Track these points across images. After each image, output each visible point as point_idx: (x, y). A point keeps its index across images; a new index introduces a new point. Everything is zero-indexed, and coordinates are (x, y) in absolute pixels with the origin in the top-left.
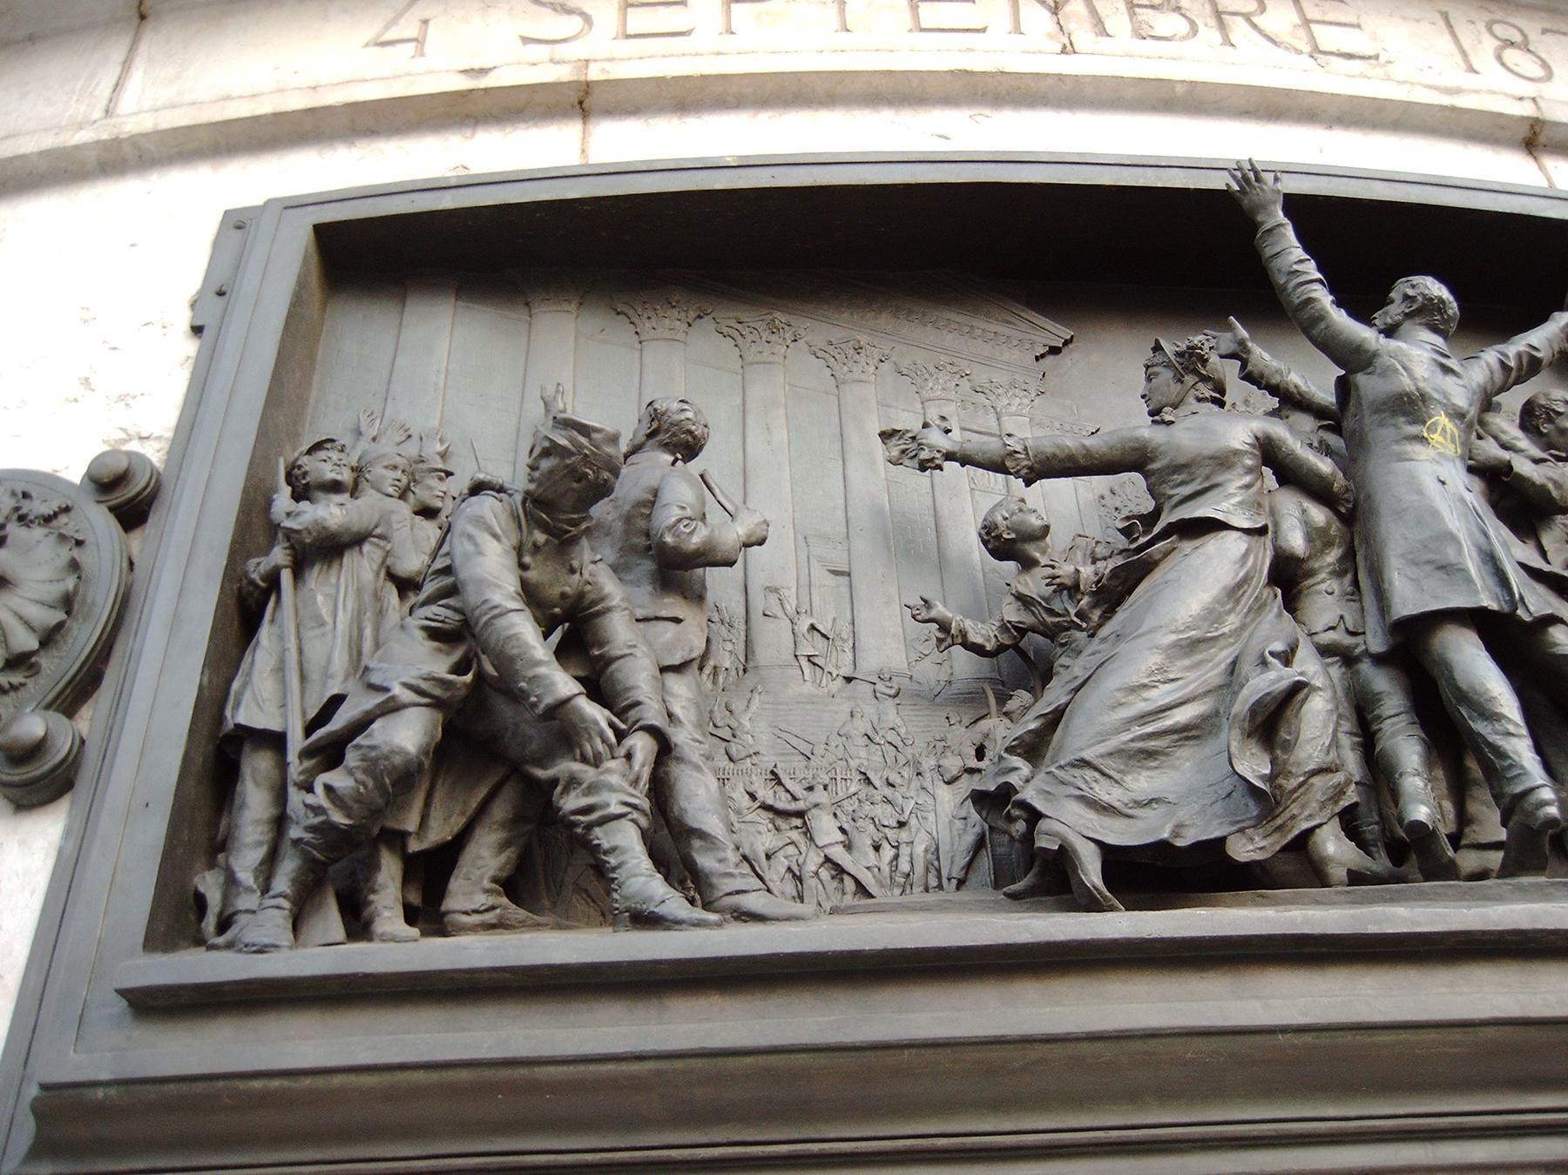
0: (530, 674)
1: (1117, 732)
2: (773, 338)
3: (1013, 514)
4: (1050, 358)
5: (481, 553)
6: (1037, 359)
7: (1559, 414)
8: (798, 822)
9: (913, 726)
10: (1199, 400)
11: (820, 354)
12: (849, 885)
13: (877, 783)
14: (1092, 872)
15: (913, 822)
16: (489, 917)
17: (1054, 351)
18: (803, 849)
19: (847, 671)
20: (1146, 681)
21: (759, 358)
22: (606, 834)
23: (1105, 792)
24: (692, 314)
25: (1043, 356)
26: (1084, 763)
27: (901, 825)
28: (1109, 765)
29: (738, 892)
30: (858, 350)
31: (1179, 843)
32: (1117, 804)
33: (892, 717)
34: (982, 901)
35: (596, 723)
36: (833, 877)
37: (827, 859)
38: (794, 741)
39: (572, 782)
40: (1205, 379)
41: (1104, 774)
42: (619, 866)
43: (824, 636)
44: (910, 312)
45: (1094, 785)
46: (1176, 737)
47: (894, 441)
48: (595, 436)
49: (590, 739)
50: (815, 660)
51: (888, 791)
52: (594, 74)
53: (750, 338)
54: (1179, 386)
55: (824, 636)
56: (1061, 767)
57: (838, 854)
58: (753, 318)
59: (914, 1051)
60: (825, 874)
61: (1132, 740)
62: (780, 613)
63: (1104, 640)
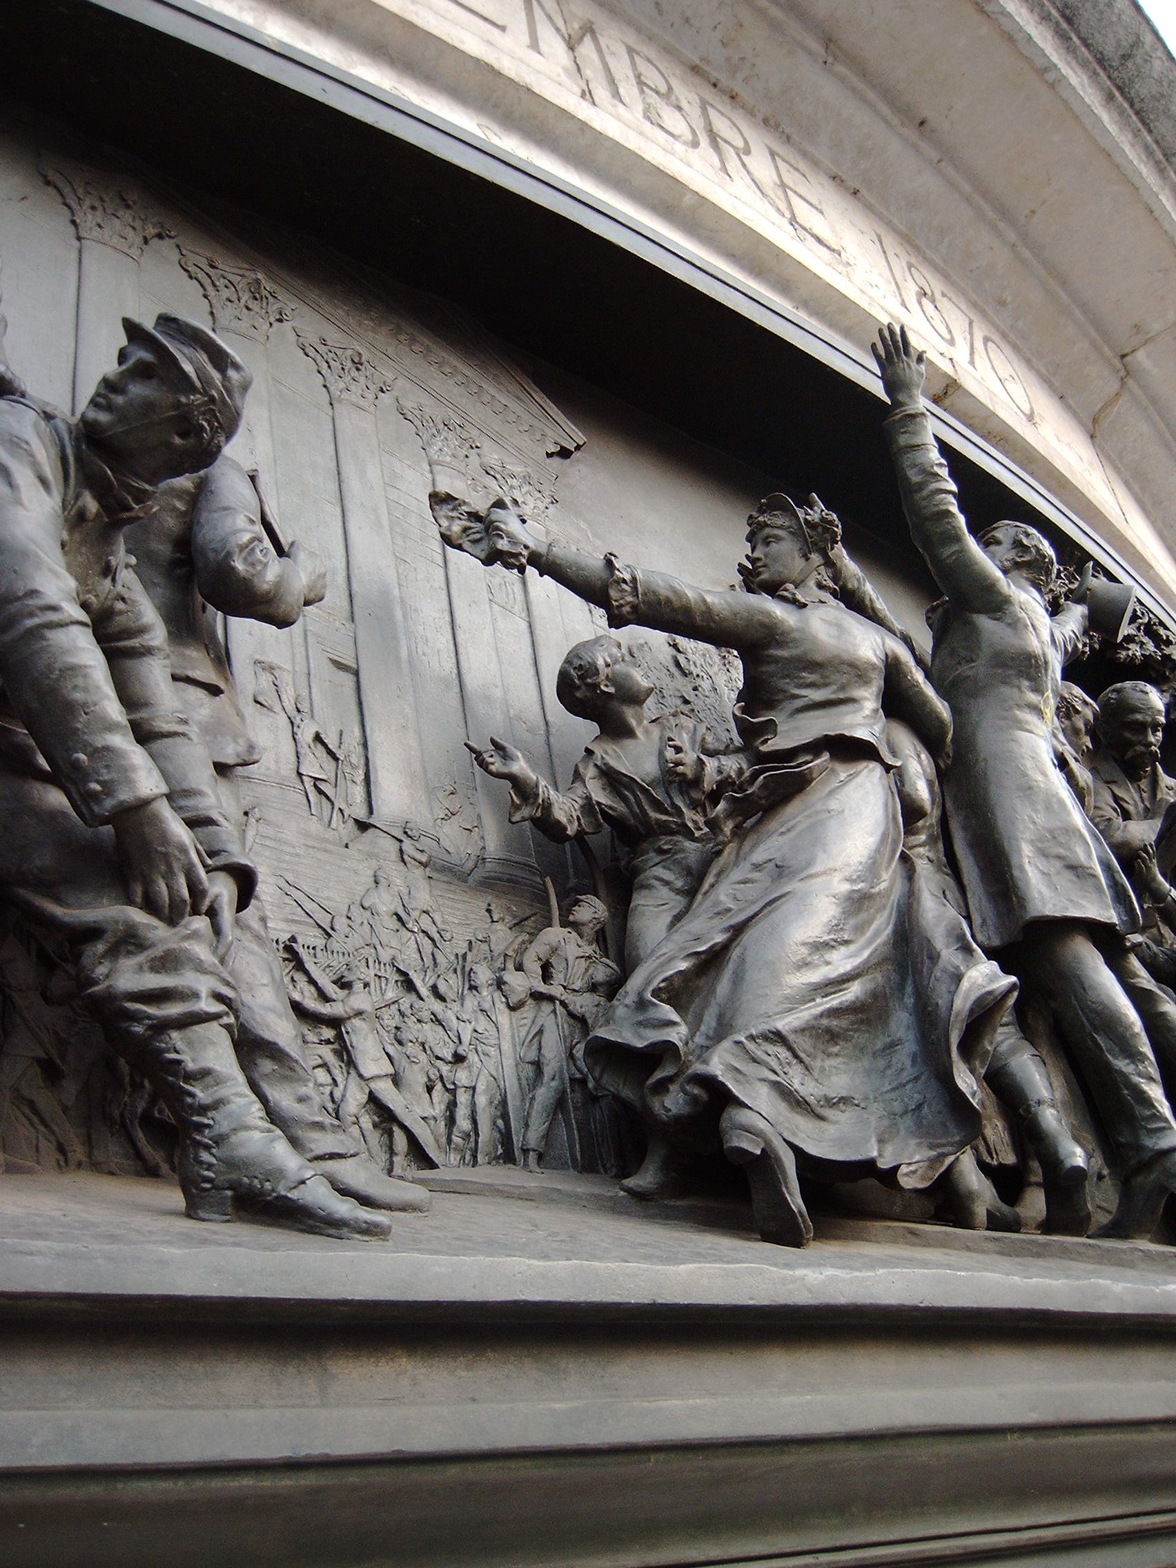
2: (255, 305)
3: (616, 662)
4: (557, 460)
5: (18, 502)
7: (1077, 712)
8: (328, 1033)
9: (464, 919)
11: (312, 353)
13: (424, 991)
15: (473, 1058)
17: (564, 453)
18: (339, 1079)
19: (361, 813)
21: (235, 324)
22: (190, 1044)
26: (778, 1037)
27: (459, 1059)
28: (803, 1044)
29: (333, 1156)
30: (358, 365)
32: (811, 1100)
33: (423, 896)
34: (598, 1197)
35: (183, 849)
36: (375, 1126)
37: (373, 1099)
38: (309, 905)
39: (130, 941)
42: (217, 1104)
43: (330, 753)
44: (413, 340)
47: (445, 510)
48: (232, 373)
49: (169, 876)
50: (322, 786)
51: (437, 1006)
53: (226, 293)
55: (330, 753)
56: (752, 1038)
57: (385, 1090)
58: (230, 268)
59: (662, 1456)
60: (366, 1121)
62: (278, 708)
63: (757, 867)
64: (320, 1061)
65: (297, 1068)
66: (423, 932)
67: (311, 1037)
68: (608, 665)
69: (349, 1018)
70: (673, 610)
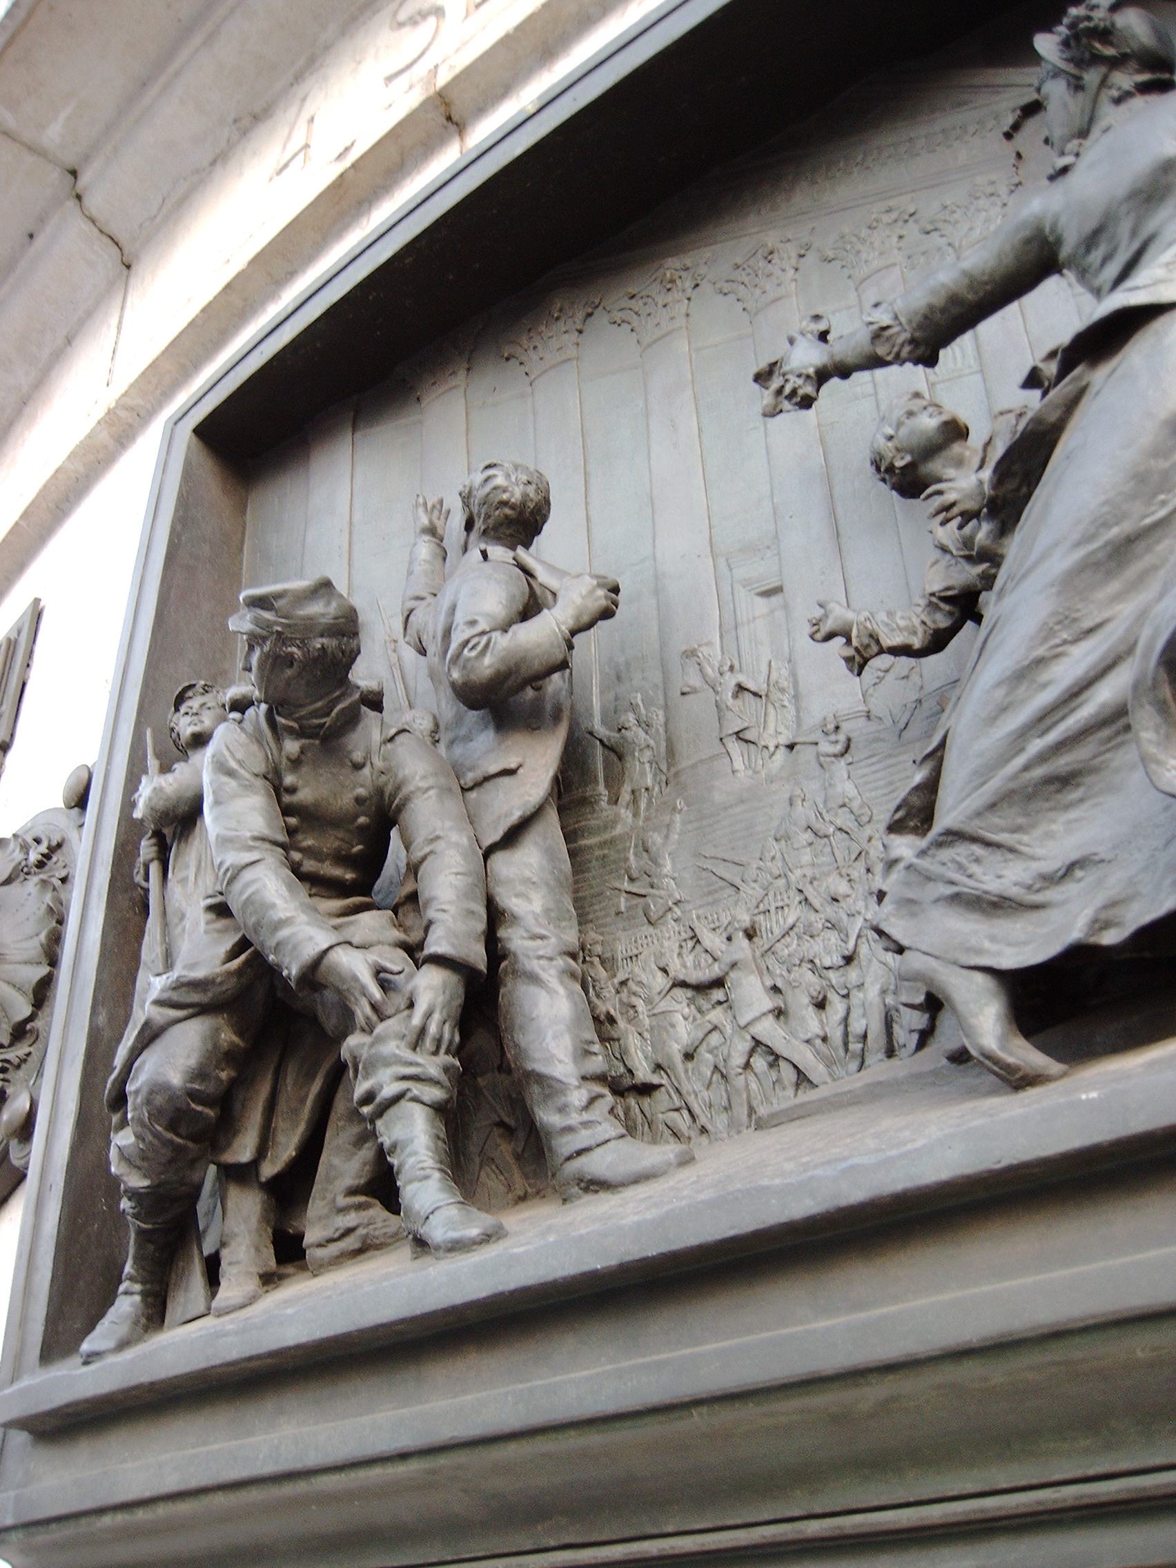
0: (271, 943)
1: (1005, 759)
2: (669, 298)
3: (899, 424)
6: (1008, 136)
10: (1118, 101)
11: (727, 287)
12: (788, 1074)
13: (816, 903)
14: (985, 1020)
16: (351, 1243)
20: (1041, 652)
23: (1001, 876)
24: (580, 315)
25: (1016, 127)
27: (848, 960)
29: (579, 1153)
31: (1110, 938)
32: (1015, 892)
40: (1116, 63)
41: (988, 844)
43: (755, 694)
45: (974, 869)
46: (1106, 732)
48: (279, 604)
51: (830, 911)
52: (442, 80)
54: (1080, 95)
55: (755, 694)
57: (769, 1030)
60: (759, 1063)
61: (1026, 768)
64: (710, 1027)
65: (554, 1084)
66: (840, 829)
67: (705, 1005)
68: (890, 438)
69: (727, 973)
70: (943, 311)
